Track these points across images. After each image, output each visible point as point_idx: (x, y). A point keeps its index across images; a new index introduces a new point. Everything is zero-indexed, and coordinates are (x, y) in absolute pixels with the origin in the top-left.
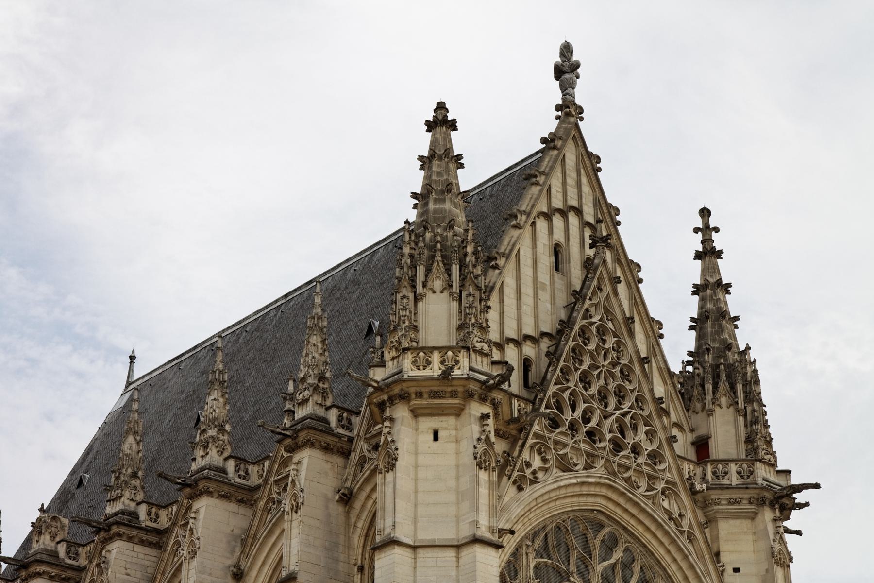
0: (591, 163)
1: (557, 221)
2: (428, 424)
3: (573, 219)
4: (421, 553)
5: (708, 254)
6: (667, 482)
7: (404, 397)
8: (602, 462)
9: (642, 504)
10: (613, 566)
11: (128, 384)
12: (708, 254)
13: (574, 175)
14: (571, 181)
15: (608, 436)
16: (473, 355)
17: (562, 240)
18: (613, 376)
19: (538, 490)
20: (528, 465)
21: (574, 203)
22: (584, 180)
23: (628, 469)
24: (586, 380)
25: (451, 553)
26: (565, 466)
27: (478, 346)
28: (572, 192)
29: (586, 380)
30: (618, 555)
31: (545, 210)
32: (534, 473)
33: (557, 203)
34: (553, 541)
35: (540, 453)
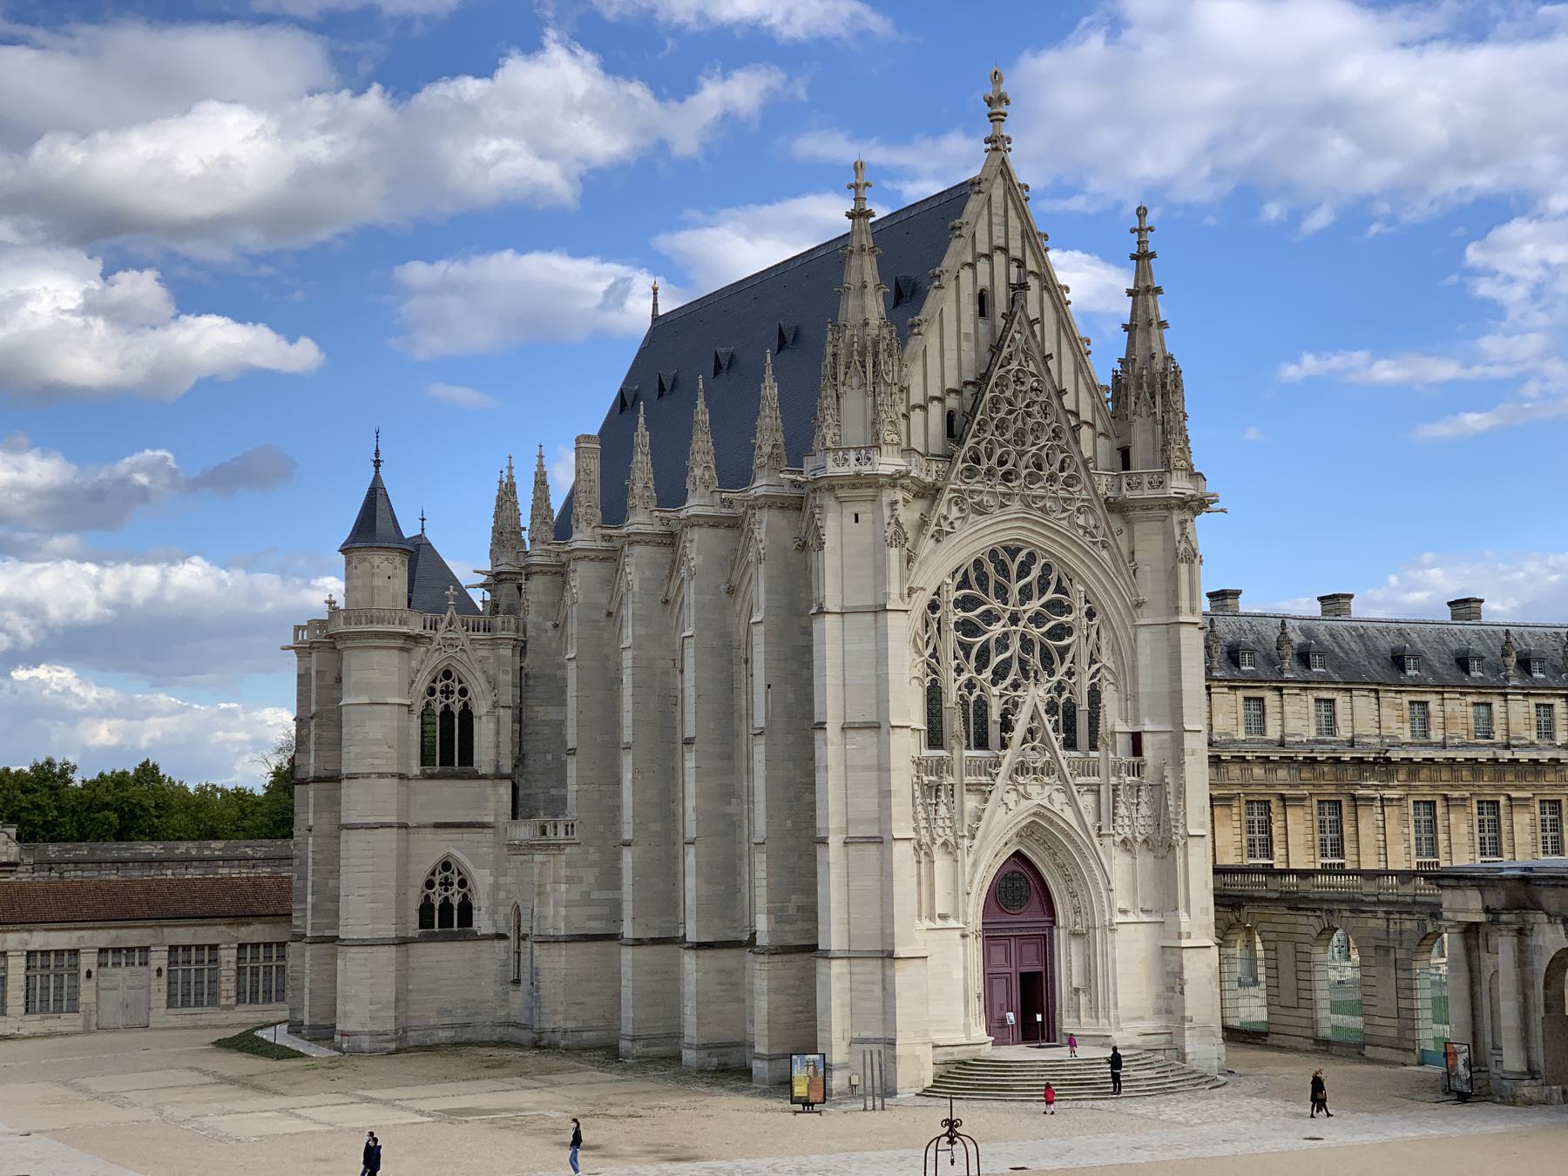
1: (983, 266)
2: (850, 509)
3: (999, 258)
4: (847, 617)
7: (832, 488)
11: (655, 318)
13: (1001, 212)
15: (1024, 473)
17: (987, 284)
18: (1029, 415)
20: (946, 518)
21: (1001, 242)
22: (1012, 213)
25: (870, 617)
26: (980, 509)
28: (998, 231)
29: (1002, 426)
30: (1035, 572)
31: (970, 260)
33: (983, 248)
34: (972, 576)
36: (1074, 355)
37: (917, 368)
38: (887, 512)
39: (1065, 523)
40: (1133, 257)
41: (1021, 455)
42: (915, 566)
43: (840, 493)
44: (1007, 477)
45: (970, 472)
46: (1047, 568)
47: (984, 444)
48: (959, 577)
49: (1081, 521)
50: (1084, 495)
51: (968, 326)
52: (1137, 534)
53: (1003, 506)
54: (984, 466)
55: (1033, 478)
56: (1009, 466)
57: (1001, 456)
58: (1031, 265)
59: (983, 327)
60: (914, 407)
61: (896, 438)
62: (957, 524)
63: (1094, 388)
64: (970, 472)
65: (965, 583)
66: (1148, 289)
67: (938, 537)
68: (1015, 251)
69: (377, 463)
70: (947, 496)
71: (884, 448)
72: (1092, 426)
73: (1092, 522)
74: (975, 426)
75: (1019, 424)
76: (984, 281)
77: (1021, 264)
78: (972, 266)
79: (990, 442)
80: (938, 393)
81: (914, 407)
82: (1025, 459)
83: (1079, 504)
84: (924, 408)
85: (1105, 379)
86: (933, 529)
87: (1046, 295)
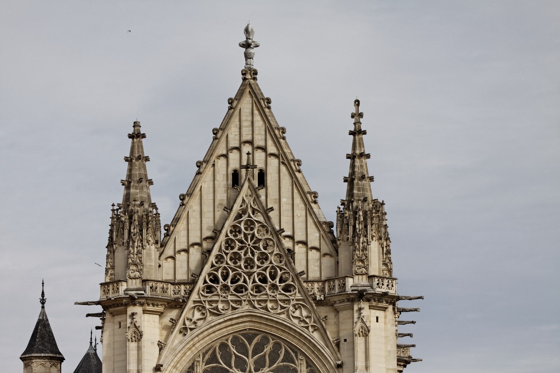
0: (262, 104)
1: (234, 156)
2: (118, 319)
5: (357, 132)
6: (297, 300)
8: (247, 302)
9: (275, 319)
10: (264, 356)
12: (357, 132)
13: (250, 118)
14: (246, 124)
15: (250, 286)
16: (130, 281)
19: (196, 332)
21: (249, 138)
22: (258, 118)
23: (266, 301)
24: (236, 258)
26: (216, 313)
27: (132, 275)
30: (268, 349)
32: (195, 323)
33: (234, 143)
35: (199, 310)
36: (306, 205)
37: (181, 225)
38: (129, 320)
39: (283, 316)
40: (351, 133)
41: (250, 275)
42: (165, 352)
43: (110, 310)
44: (239, 289)
45: (210, 290)
46: (277, 346)
47: (220, 271)
48: (207, 357)
49: (297, 314)
50: (298, 296)
51: (222, 196)
52: (341, 319)
53: (234, 308)
54: (218, 287)
55: (258, 289)
56: (240, 283)
57: (235, 276)
58: (272, 149)
59: (232, 193)
60: (179, 252)
61: (137, 274)
62: (200, 323)
63: (319, 224)
64: (210, 290)
65: (214, 359)
66: (362, 155)
67: (184, 330)
68: (259, 141)
69: (43, 302)
70: (190, 304)
71: (130, 281)
72: (318, 249)
73: (305, 313)
74: (212, 259)
75: (249, 254)
76: (234, 164)
77: (264, 149)
78: (226, 156)
79: (225, 268)
80: (198, 241)
81: (179, 252)
82: (252, 277)
83: (295, 302)
84: (187, 251)
85: (333, 218)
86: (179, 325)
87: (283, 168)
